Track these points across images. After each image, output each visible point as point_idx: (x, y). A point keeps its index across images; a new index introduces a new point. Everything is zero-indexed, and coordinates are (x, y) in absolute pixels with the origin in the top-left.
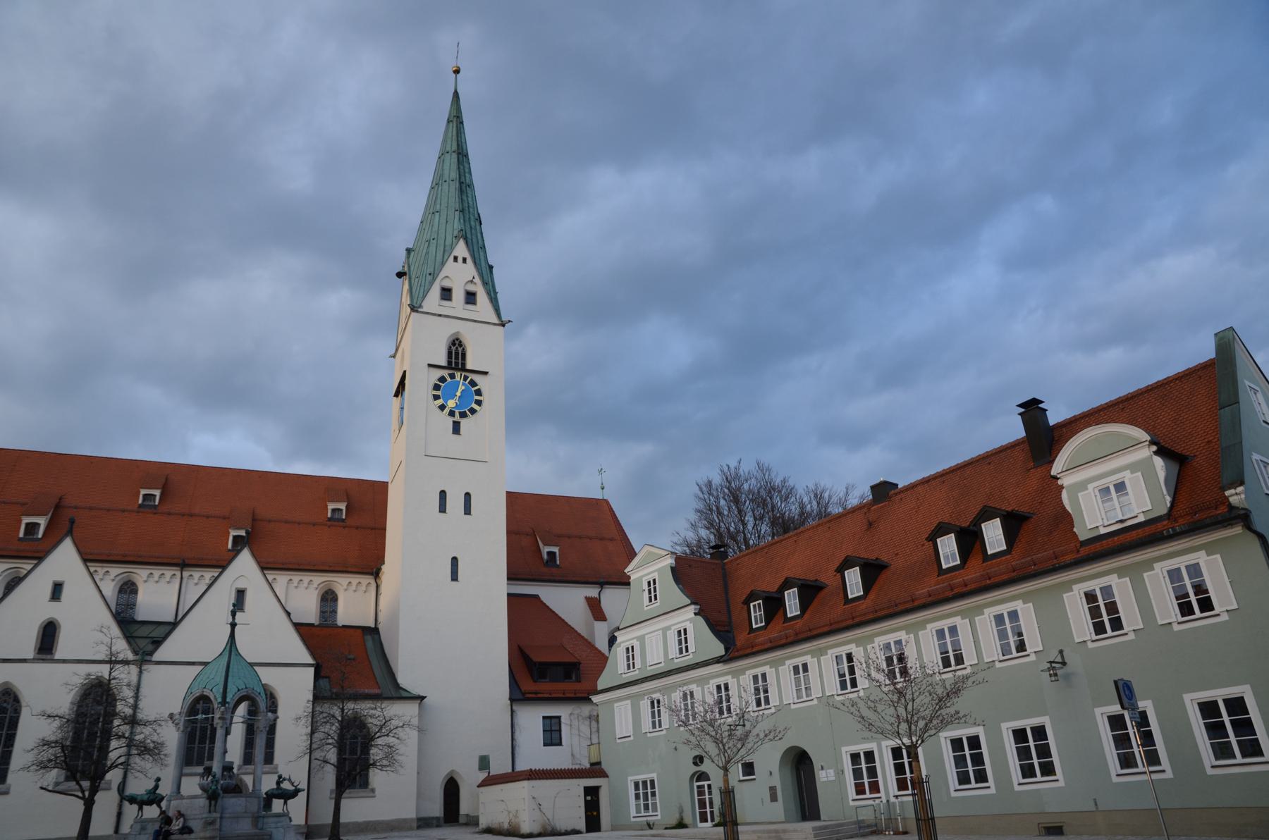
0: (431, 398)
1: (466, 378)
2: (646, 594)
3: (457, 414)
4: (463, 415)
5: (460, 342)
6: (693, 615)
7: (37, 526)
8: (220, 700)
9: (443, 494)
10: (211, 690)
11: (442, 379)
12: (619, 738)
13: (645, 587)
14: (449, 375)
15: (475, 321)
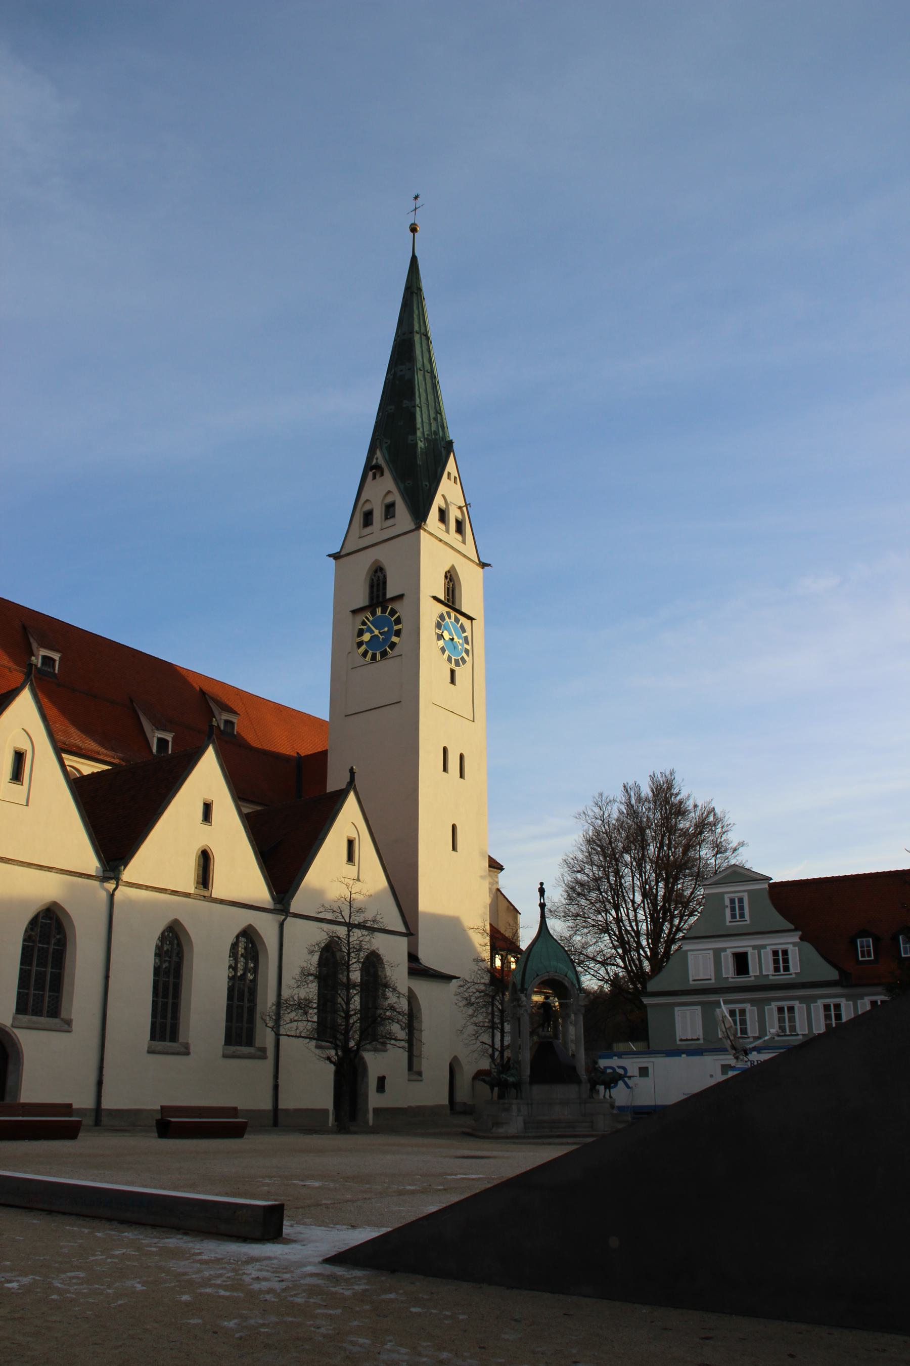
0: (435, 637)
1: (457, 620)
2: (728, 912)
4: (457, 664)
5: (451, 576)
6: (799, 940)
8: (577, 987)
9: (445, 750)
10: (566, 976)
11: (442, 617)
12: (681, 1040)
13: (727, 902)
15: (465, 556)
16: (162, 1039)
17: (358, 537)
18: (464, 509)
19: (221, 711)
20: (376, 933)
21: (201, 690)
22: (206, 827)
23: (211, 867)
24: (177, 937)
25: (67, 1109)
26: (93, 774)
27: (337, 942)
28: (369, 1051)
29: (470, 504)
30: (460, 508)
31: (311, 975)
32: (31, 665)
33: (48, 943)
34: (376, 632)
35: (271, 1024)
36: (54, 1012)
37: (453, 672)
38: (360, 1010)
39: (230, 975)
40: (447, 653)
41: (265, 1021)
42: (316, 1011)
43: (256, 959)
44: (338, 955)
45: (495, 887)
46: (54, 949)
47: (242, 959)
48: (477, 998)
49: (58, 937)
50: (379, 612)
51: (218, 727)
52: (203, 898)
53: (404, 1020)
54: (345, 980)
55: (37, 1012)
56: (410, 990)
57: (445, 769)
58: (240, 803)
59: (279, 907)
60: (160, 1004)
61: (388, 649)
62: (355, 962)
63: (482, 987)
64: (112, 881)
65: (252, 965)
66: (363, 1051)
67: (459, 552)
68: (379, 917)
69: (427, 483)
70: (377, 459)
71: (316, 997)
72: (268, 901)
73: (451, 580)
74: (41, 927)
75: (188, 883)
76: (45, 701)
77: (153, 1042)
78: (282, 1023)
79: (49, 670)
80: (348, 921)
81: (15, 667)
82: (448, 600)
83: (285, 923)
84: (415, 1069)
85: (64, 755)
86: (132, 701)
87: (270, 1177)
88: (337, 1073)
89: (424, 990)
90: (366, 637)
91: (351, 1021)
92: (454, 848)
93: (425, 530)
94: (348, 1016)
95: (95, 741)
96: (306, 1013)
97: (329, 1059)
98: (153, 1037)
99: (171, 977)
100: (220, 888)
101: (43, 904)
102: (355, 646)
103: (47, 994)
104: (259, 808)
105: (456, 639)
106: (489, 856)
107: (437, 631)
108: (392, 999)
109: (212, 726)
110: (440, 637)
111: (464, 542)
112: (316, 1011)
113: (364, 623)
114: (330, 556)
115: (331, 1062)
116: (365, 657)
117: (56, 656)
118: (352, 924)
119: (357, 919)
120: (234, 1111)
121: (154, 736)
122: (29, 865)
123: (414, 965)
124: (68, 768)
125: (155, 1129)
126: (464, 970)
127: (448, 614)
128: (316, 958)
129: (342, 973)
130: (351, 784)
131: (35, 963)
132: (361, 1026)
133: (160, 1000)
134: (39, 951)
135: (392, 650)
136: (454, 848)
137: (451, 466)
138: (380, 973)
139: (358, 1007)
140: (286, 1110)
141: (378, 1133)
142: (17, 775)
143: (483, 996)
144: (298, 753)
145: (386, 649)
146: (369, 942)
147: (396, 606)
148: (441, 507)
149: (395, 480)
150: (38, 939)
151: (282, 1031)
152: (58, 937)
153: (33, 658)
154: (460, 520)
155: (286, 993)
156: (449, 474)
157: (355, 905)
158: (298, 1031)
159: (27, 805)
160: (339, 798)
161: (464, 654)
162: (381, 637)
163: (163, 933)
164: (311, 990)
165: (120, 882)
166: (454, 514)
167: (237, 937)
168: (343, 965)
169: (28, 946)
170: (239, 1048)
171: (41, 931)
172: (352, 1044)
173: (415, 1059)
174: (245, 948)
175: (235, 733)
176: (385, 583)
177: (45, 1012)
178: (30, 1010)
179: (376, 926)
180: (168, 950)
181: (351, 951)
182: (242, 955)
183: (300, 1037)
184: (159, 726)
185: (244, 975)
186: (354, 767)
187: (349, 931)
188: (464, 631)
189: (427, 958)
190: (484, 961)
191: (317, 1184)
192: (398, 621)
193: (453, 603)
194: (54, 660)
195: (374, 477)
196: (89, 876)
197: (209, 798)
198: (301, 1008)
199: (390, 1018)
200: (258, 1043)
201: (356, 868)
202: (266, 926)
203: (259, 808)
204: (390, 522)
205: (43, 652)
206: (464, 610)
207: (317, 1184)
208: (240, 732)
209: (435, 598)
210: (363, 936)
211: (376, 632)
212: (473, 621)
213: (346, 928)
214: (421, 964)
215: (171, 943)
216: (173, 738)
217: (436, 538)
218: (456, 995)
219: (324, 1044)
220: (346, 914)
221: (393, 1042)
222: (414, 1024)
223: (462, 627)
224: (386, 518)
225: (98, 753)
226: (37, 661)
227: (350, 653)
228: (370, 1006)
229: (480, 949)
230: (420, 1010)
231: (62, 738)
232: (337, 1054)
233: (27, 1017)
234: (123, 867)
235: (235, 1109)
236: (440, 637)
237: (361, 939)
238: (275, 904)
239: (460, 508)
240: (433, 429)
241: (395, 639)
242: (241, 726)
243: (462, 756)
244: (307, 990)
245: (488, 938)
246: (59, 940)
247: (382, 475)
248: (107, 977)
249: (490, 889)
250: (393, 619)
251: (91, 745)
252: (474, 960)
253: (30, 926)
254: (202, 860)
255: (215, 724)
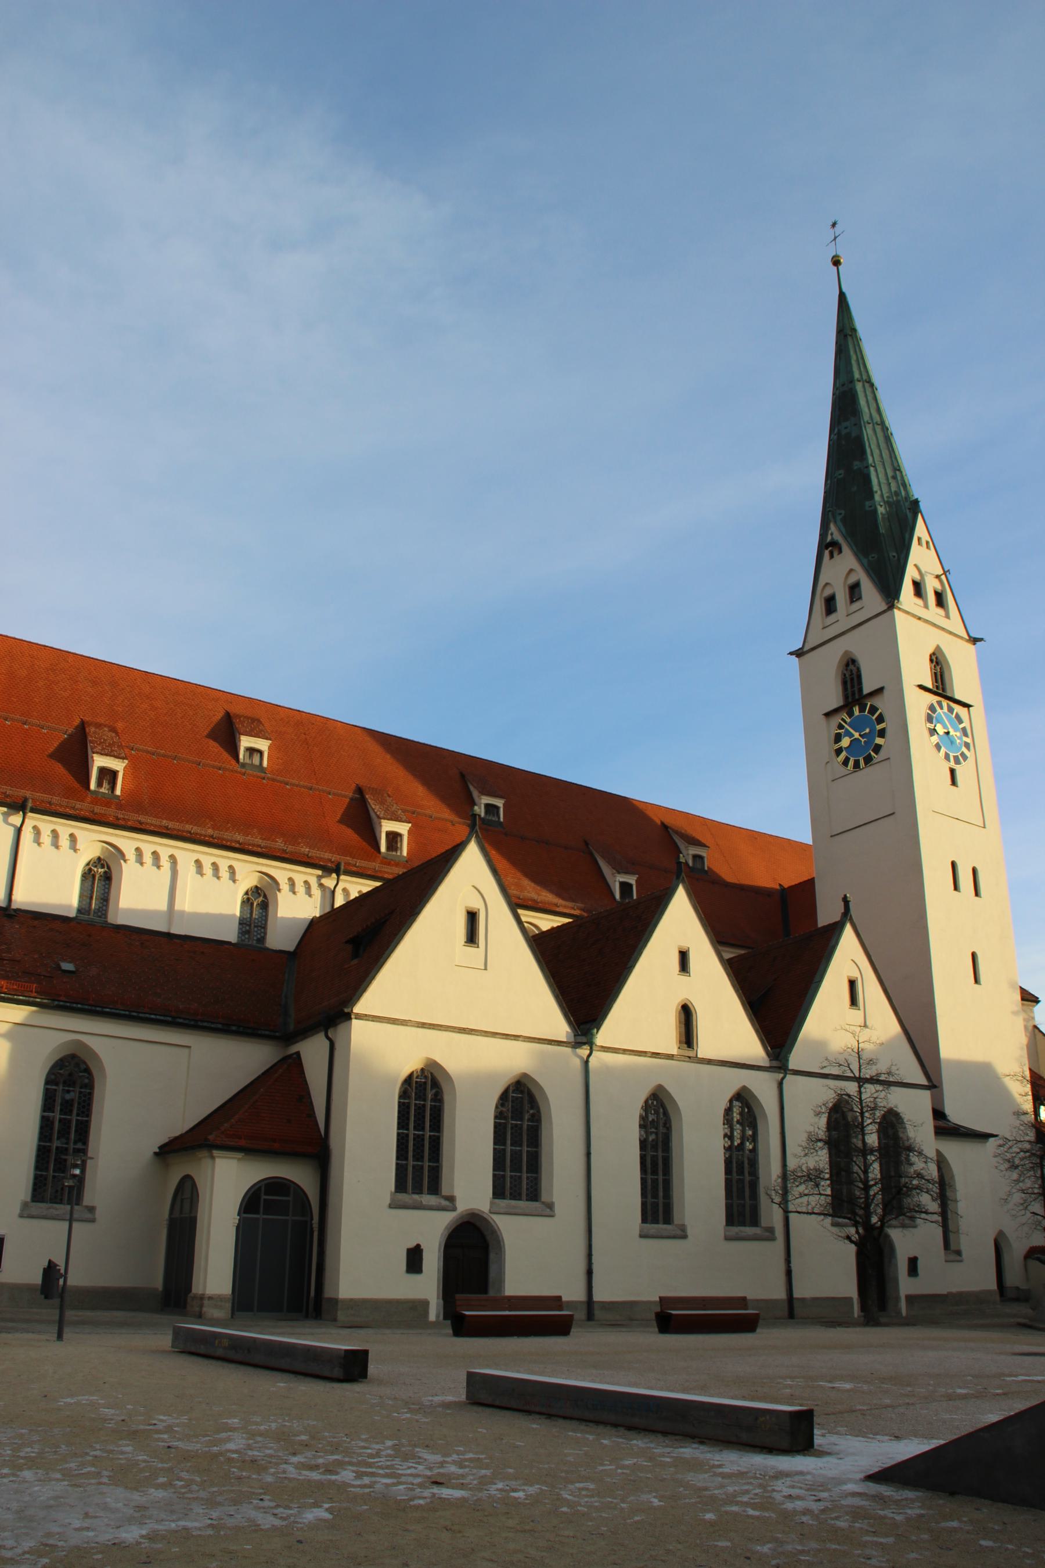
0: (926, 733)
1: (951, 710)
3: (952, 759)
4: (957, 761)
5: (937, 658)
7: (399, 839)
11: (932, 708)
14: (937, 702)
15: (951, 633)
16: (655, 1221)
17: (821, 627)
18: (943, 577)
19: (687, 844)
20: (892, 1088)
21: (662, 823)
22: (684, 978)
23: (694, 1023)
24: (663, 1106)
25: (556, 1301)
26: (553, 929)
27: (847, 1102)
28: (895, 1227)
29: (948, 571)
30: (938, 577)
31: (820, 1140)
32: (474, 816)
33: (521, 1119)
34: (856, 735)
35: (777, 1199)
36: (534, 1195)
37: (952, 772)
38: (880, 1180)
39: (726, 1145)
40: (943, 750)
41: (769, 1196)
42: (828, 1182)
43: (754, 1126)
44: (850, 1116)
45: (1030, 1025)
46: (528, 1125)
47: (738, 1126)
48: (1022, 1159)
49: (531, 1112)
50: (856, 711)
51: (686, 863)
52: (688, 1059)
53: (935, 1189)
54: (860, 1144)
55: (516, 1196)
56: (938, 1152)
57: (956, 888)
58: (720, 948)
59: (775, 1063)
60: (649, 1182)
61: (872, 753)
62: (871, 1123)
63: (1027, 1146)
64: (585, 1047)
65: (750, 1133)
66: (889, 1227)
67: (943, 629)
68: (894, 1069)
69: (894, 554)
70: (832, 534)
71: (827, 1166)
72: (763, 1058)
73: (937, 663)
74: (512, 1102)
75: (668, 1041)
76: (493, 853)
77: (645, 1225)
78: (790, 1197)
79: (494, 819)
80: (857, 1075)
81: (457, 819)
82: (937, 687)
83: (785, 1081)
84: (953, 1247)
85: (520, 911)
86: (587, 844)
87: (792, 1378)
88: (860, 1255)
89: (954, 1151)
90: (845, 742)
91: (872, 1193)
92: (977, 980)
93: (899, 609)
94: (867, 1188)
95: (551, 891)
96: (817, 1185)
97: (848, 1238)
98: (644, 1220)
99: (660, 1150)
100: (707, 1045)
101: (514, 1074)
102: (833, 754)
103: (525, 1175)
104: (743, 952)
105: (952, 733)
106: (1021, 987)
107: (929, 725)
108: (918, 1164)
109: (679, 863)
110: (933, 732)
111: (947, 616)
112: (828, 1182)
113: (841, 727)
114: (791, 654)
115: (852, 1241)
116: (847, 766)
117: (499, 803)
118: (863, 1079)
119: (867, 1073)
120: (742, 1302)
121: (616, 881)
122: (494, 1034)
123: (941, 1123)
124: (526, 925)
125: (655, 1323)
126: (1003, 1126)
127: (940, 704)
128: (823, 1120)
129: (856, 1137)
130: (846, 914)
131: (509, 1142)
132: (883, 1199)
133: (649, 1177)
134: (512, 1128)
135: (877, 753)
136: (977, 980)
137: (920, 530)
138: (901, 1135)
139: (879, 1176)
140: (803, 1300)
141: (914, 1325)
142: (472, 938)
143: (1029, 1156)
144: (780, 885)
145: (870, 753)
146: (886, 1097)
147: (876, 701)
148: (915, 579)
149: (856, 555)
150: (510, 1115)
151: (791, 1207)
152: (531, 1112)
153: (476, 808)
154: (940, 591)
155: (792, 1164)
156: (919, 539)
157: (865, 1056)
158: (810, 1207)
159: (486, 969)
160: (833, 932)
161: (964, 750)
162: (863, 740)
163: (646, 1102)
164: (821, 1158)
165: (594, 1048)
166: (931, 585)
167: (731, 1101)
168: (857, 1127)
169: (500, 1123)
170: (742, 1228)
171: (512, 1107)
172: (874, 1219)
173: (952, 1236)
174: (741, 1114)
175: (706, 868)
176: (859, 677)
177: (524, 1196)
178: (508, 1193)
179: (891, 1080)
180: (653, 1120)
181: (865, 1109)
182: (738, 1122)
183: (813, 1213)
184: (620, 869)
185: (741, 1145)
186: (848, 895)
187: (860, 1087)
188: (960, 721)
189: (955, 1115)
190: (1026, 1113)
191: (848, 1386)
192: (880, 719)
193: (944, 690)
194: (497, 808)
195: (832, 556)
196: (559, 1043)
197: (685, 945)
198: (811, 1180)
199: (917, 1187)
200: (764, 1222)
201: (861, 1012)
202: (763, 1086)
203: (743, 952)
204: (856, 606)
205: (486, 800)
206: (957, 697)
207: (848, 1386)
208: (711, 866)
209: (921, 687)
210: (877, 1091)
211: (856, 735)
212: (971, 708)
213: (856, 1084)
214: (950, 1122)
215: (657, 1113)
216: (636, 881)
217: (914, 616)
218: (995, 1156)
219: (840, 1220)
220: (855, 1067)
221: (923, 1216)
222: (947, 1194)
223: (958, 717)
224: (852, 602)
225: (556, 905)
226: (480, 810)
227: (828, 762)
228: (893, 1174)
229: (1019, 1099)
230: (952, 1177)
231: (515, 892)
232: (857, 1232)
233: (505, 1201)
234: (595, 1030)
235: (744, 1299)
236: (933, 732)
237: (875, 1096)
238: (770, 1060)
239: (938, 577)
240: (893, 489)
241: (879, 741)
242: (713, 861)
243: (974, 871)
244: (817, 1158)
245: (1029, 1086)
246: (533, 1115)
247: (840, 551)
248: (588, 1154)
249: (1026, 1027)
250: (874, 718)
251: (547, 897)
252: (1014, 1113)
253: (501, 1102)
254: (683, 1016)
255: (682, 860)
